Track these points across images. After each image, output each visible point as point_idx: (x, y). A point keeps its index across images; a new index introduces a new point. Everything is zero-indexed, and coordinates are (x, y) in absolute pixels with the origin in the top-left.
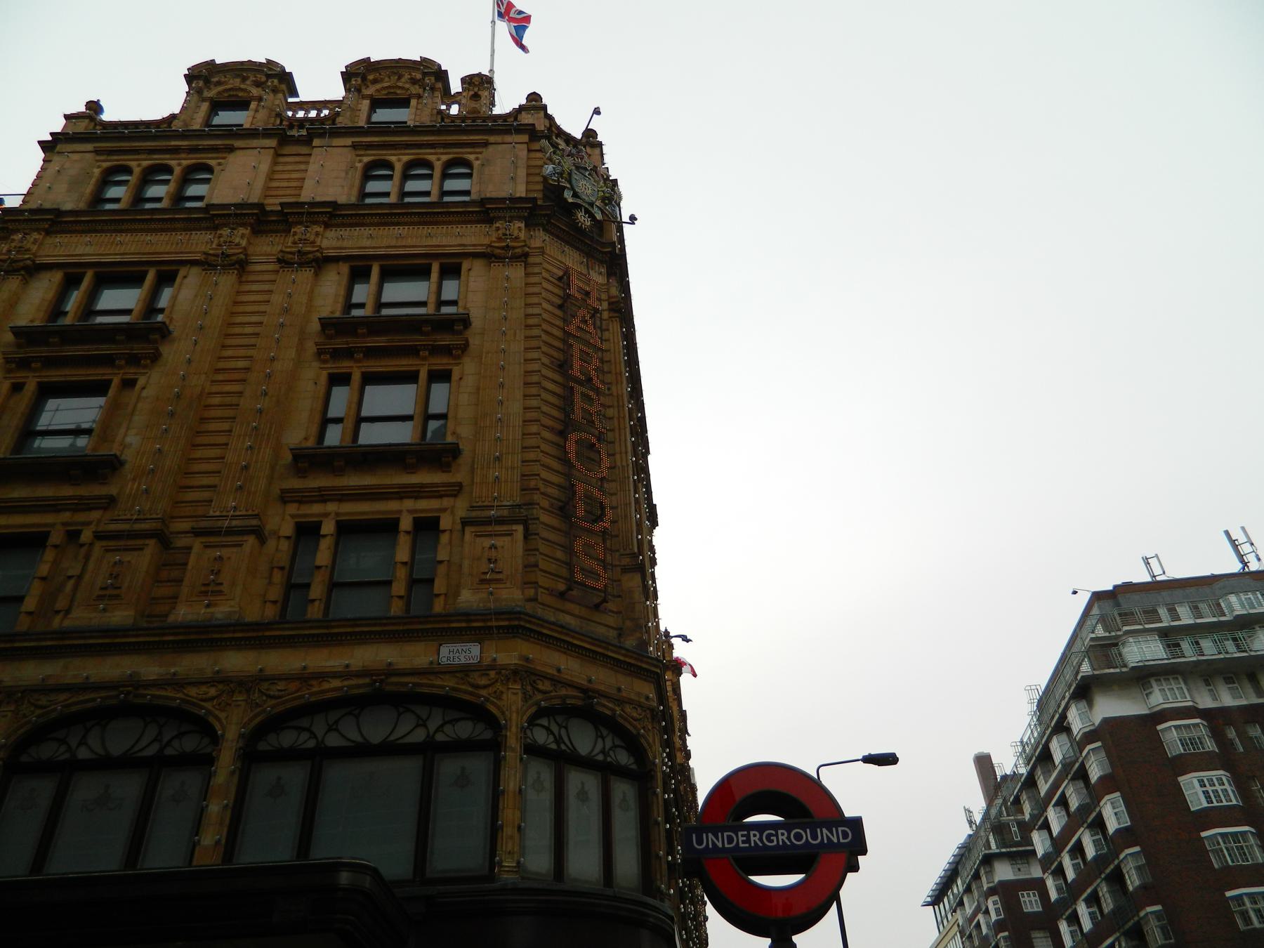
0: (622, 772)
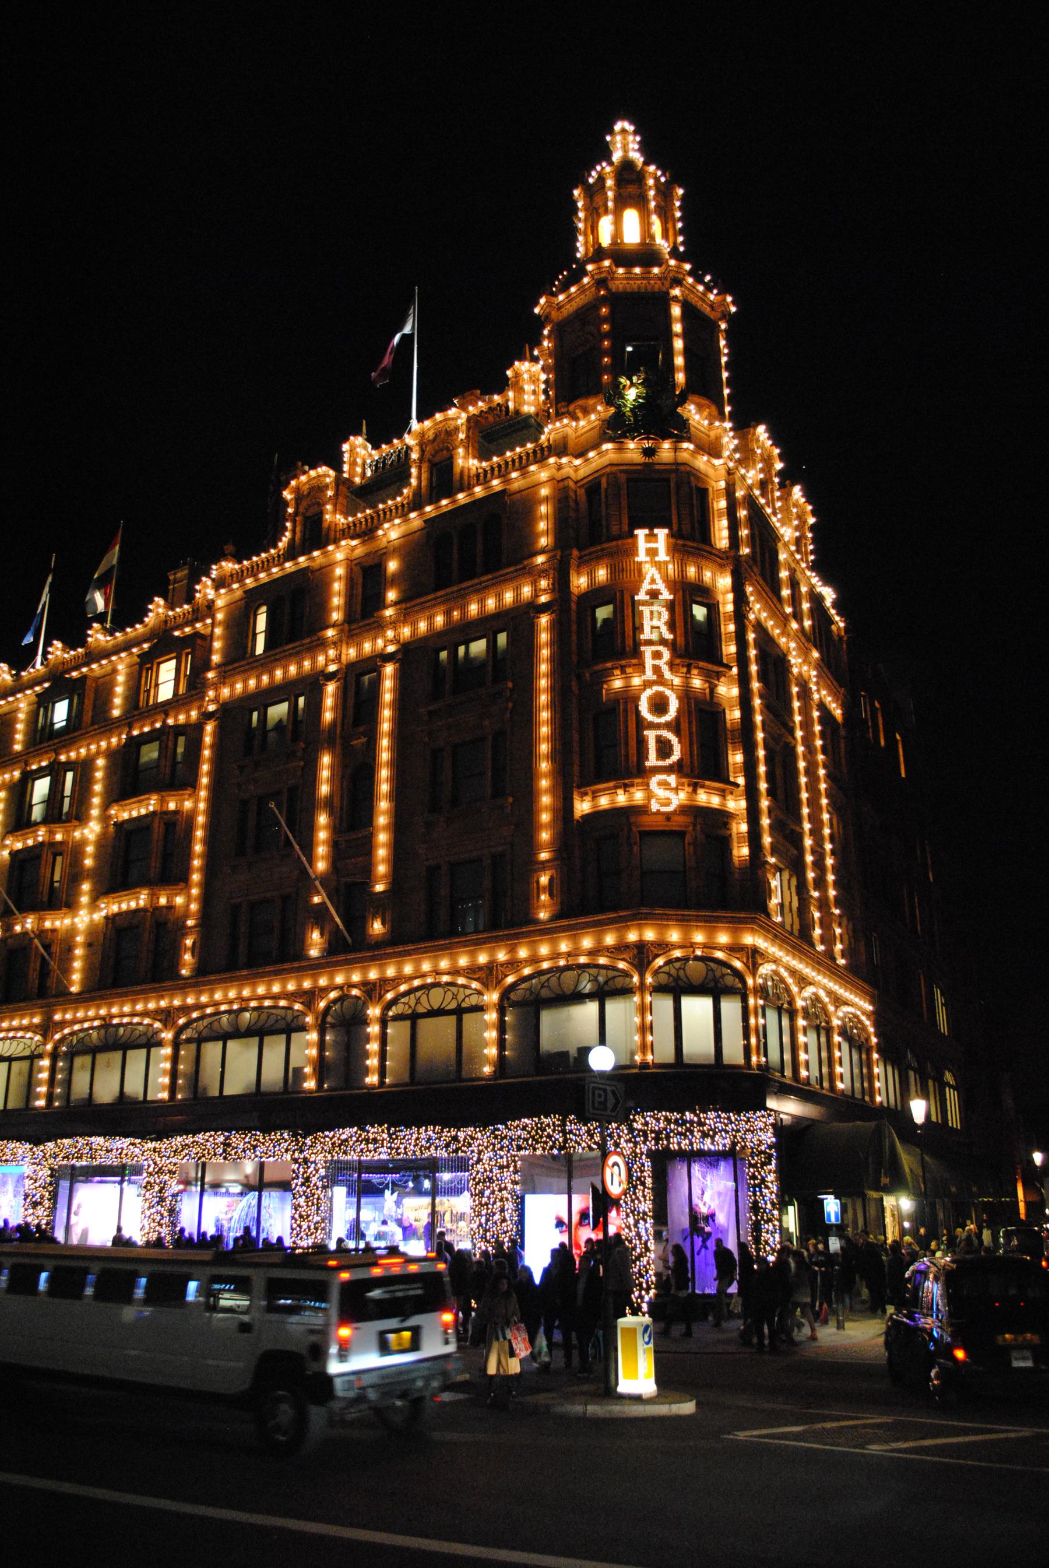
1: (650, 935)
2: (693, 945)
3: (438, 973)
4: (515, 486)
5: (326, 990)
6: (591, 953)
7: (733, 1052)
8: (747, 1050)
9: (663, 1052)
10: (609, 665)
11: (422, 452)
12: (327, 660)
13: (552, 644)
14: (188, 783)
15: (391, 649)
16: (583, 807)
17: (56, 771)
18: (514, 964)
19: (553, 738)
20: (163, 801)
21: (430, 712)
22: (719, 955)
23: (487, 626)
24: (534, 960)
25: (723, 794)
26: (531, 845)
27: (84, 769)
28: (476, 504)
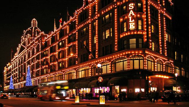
1: (129, 53)
2: (136, 53)
3: (104, 60)
5: (91, 64)
6: (122, 56)
7: (142, 67)
9: (131, 68)
10: (125, 15)
12: (89, 21)
14: (75, 40)
17: (62, 41)
18: (113, 58)
19: (117, 27)
20: (73, 43)
22: (140, 54)
24: (115, 57)
25: (142, 32)
26: (115, 42)
27: (65, 40)
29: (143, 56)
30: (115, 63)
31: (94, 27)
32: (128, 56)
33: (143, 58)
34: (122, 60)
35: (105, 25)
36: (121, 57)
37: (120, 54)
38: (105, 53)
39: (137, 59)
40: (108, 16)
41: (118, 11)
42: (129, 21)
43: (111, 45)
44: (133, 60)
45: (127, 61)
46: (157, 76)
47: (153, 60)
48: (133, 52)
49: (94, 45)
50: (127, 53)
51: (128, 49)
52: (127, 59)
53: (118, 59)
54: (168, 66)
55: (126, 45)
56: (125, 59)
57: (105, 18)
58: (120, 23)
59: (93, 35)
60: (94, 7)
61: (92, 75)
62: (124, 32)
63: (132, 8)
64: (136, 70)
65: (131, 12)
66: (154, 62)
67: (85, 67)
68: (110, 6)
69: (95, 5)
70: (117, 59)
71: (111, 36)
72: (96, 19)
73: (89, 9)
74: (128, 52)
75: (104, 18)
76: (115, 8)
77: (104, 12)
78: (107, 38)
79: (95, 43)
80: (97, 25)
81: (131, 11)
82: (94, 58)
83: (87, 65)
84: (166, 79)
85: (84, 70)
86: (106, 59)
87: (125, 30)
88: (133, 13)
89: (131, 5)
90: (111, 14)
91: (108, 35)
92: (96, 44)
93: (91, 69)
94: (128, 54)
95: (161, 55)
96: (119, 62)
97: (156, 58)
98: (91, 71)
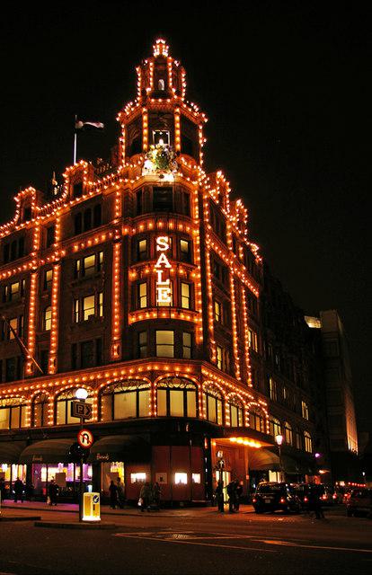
0: (191, 390)
1: (156, 368)
2: (175, 372)
4: (106, 193)
6: (133, 375)
7: (192, 413)
8: (198, 412)
9: (162, 412)
11: (70, 180)
12: (33, 265)
13: (120, 255)
15: (57, 260)
16: (132, 320)
19: (120, 293)
21: (73, 285)
22: (186, 376)
23: (94, 250)
26: (111, 334)
28: (91, 200)
29: (194, 380)
30: (112, 395)
31: (45, 282)
32: (153, 376)
33: (196, 386)
34: (134, 388)
35: (78, 282)
36: (130, 378)
37: (127, 370)
38: (78, 361)
39: (179, 389)
40: (93, 258)
41: (123, 249)
42: (156, 280)
43: (98, 340)
44: (168, 390)
45: (150, 392)
46: (233, 440)
47: (219, 396)
48: (167, 368)
49: (43, 336)
50: (149, 368)
51: (152, 356)
52: (150, 385)
53: (120, 383)
54: (255, 415)
55: (144, 345)
56: (144, 386)
57: (83, 263)
58: (129, 283)
59: (44, 305)
60: (49, 229)
61: (32, 423)
62: (139, 308)
63: (166, 249)
64: (177, 419)
65: (163, 259)
66: (223, 401)
67: (9, 398)
68: (100, 232)
69: (54, 222)
70: (117, 382)
71: (101, 315)
72: (56, 263)
73: (34, 232)
74: (152, 365)
75: (78, 262)
76: (117, 241)
77: (80, 245)
78: (86, 318)
79: (48, 328)
80: (56, 278)
81: (163, 255)
82: (41, 374)
83: (18, 392)
84: (254, 449)
85: (6, 407)
86: (84, 379)
87: (144, 303)
88: (166, 261)
89: (161, 241)
90: (101, 254)
91: (92, 312)
92: (50, 332)
93: (33, 405)
94: (152, 371)
95: (237, 384)
96: (123, 392)
97: (228, 390)
98: (33, 411)
